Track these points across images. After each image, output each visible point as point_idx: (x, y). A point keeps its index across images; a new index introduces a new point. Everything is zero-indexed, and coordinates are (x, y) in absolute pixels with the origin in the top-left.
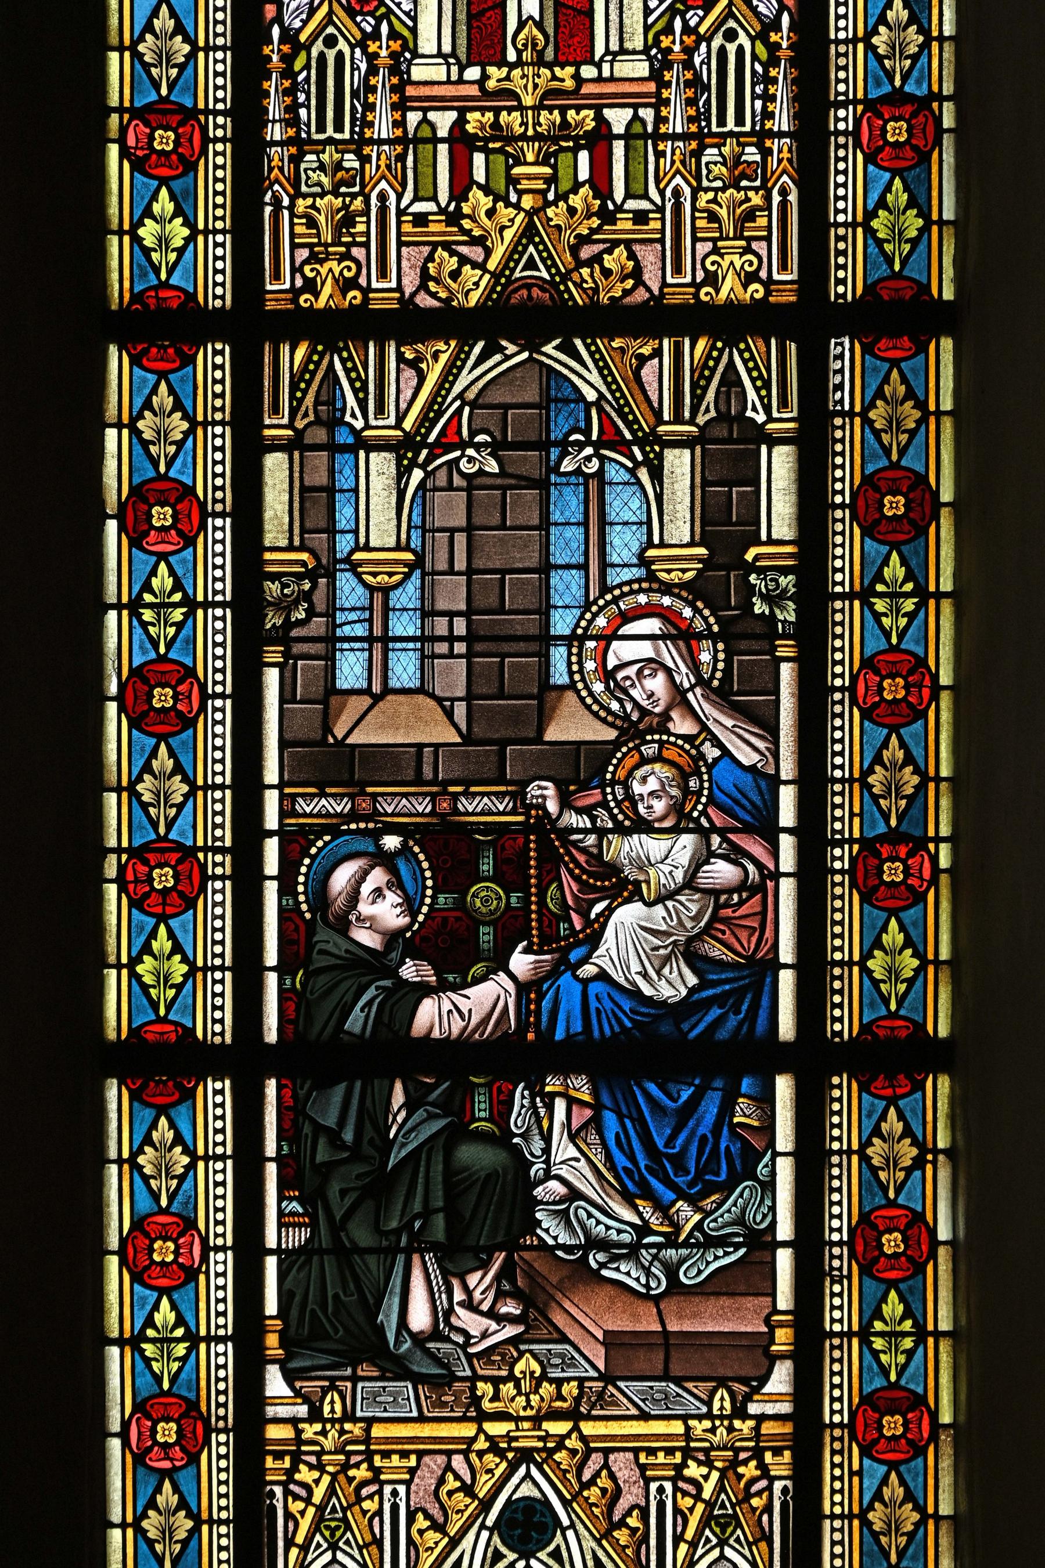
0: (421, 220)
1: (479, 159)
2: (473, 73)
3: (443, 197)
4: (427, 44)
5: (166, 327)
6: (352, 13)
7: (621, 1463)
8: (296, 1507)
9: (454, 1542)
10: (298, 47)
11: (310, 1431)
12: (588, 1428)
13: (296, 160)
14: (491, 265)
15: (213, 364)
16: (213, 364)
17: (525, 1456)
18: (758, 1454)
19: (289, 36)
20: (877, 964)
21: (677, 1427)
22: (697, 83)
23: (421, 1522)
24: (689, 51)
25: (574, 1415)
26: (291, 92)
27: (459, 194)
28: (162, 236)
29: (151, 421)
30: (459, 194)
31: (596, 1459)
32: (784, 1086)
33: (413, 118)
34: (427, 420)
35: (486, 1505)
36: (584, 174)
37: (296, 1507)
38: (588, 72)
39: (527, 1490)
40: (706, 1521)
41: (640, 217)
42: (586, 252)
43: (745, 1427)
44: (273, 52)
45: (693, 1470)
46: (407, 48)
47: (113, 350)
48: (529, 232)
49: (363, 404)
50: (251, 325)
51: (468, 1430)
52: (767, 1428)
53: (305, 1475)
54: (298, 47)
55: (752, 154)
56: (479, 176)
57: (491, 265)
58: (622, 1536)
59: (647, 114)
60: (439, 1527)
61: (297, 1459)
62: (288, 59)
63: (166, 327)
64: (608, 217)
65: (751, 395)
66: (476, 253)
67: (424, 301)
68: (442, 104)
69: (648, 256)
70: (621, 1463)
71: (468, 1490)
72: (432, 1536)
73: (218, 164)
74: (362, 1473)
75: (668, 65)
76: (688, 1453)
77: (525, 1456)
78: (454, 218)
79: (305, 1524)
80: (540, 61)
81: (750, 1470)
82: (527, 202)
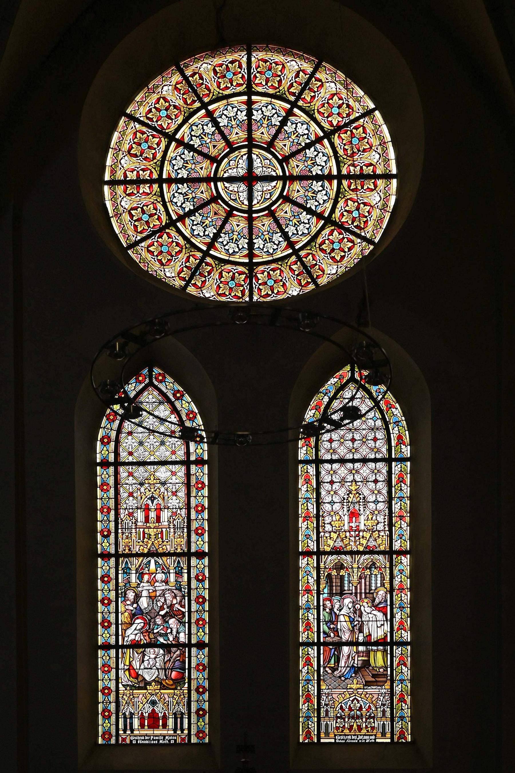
0: (139, 542)
1: (146, 535)
2: (145, 524)
3: (142, 539)
4: (139, 520)
5: (106, 556)
6: (129, 517)
7: (166, 696)
8: (123, 701)
9: (144, 705)
10: (123, 521)
11: (125, 691)
12: (161, 691)
13: (122, 535)
14: (148, 548)
15: (113, 560)
16: (113, 560)
17: (153, 694)
18: (184, 694)
19: (121, 519)
20: (199, 634)
21: (173, 691)
22: (174, 525)
23: (140, 703)
24: (173, 521)
25: (160, 690)
26: (122, 526)
27: (143, 539)
28: (104, 545)
29: (103, 567)
30: (143, 539)
31: (162, 695)
32: (187, 649)
33: (138, 530)
34: (140, 566)
35: (148, 701)
36: (160, 536)
37: (123, 701)
38: (160, 524)
39: (153, 698)
40: (177, 703)
41: (167, 542)
42: (160, 546)
43: (182, 691)
44: (120, 521)
45: (175, 697)
46: (137, 521)
47: (99, 559)
48: (153, 543)
49: (131, 565)
50: (117, 556)
51: (146, 691)
52: (185, 691)
53: (124, 697)
54: (123, 521)
55: (182, 534)
56: (146, 537)
57: (148, 548)
58: (165, 704)
59: (168, 529)
60: (142, 703)
61: (123, 695)
62: (121, 522)
63: (106, 556)
64: (163, 542)
65: (181, 564)
66: (146, 546)
67: (139, 552)
68: (141, 528)
69: (168, 547)
70: (166, 696)
71: (146, 698)
72: (141, 705)
73: (113, 535)
74: (132, 697)
75: (170, 523)
76: (174, 694)
77: (153, 694)
78: (143, 542)
79: (124, 703)
80: (154, 523)
81: (182, 697)
82: (153, 540)
